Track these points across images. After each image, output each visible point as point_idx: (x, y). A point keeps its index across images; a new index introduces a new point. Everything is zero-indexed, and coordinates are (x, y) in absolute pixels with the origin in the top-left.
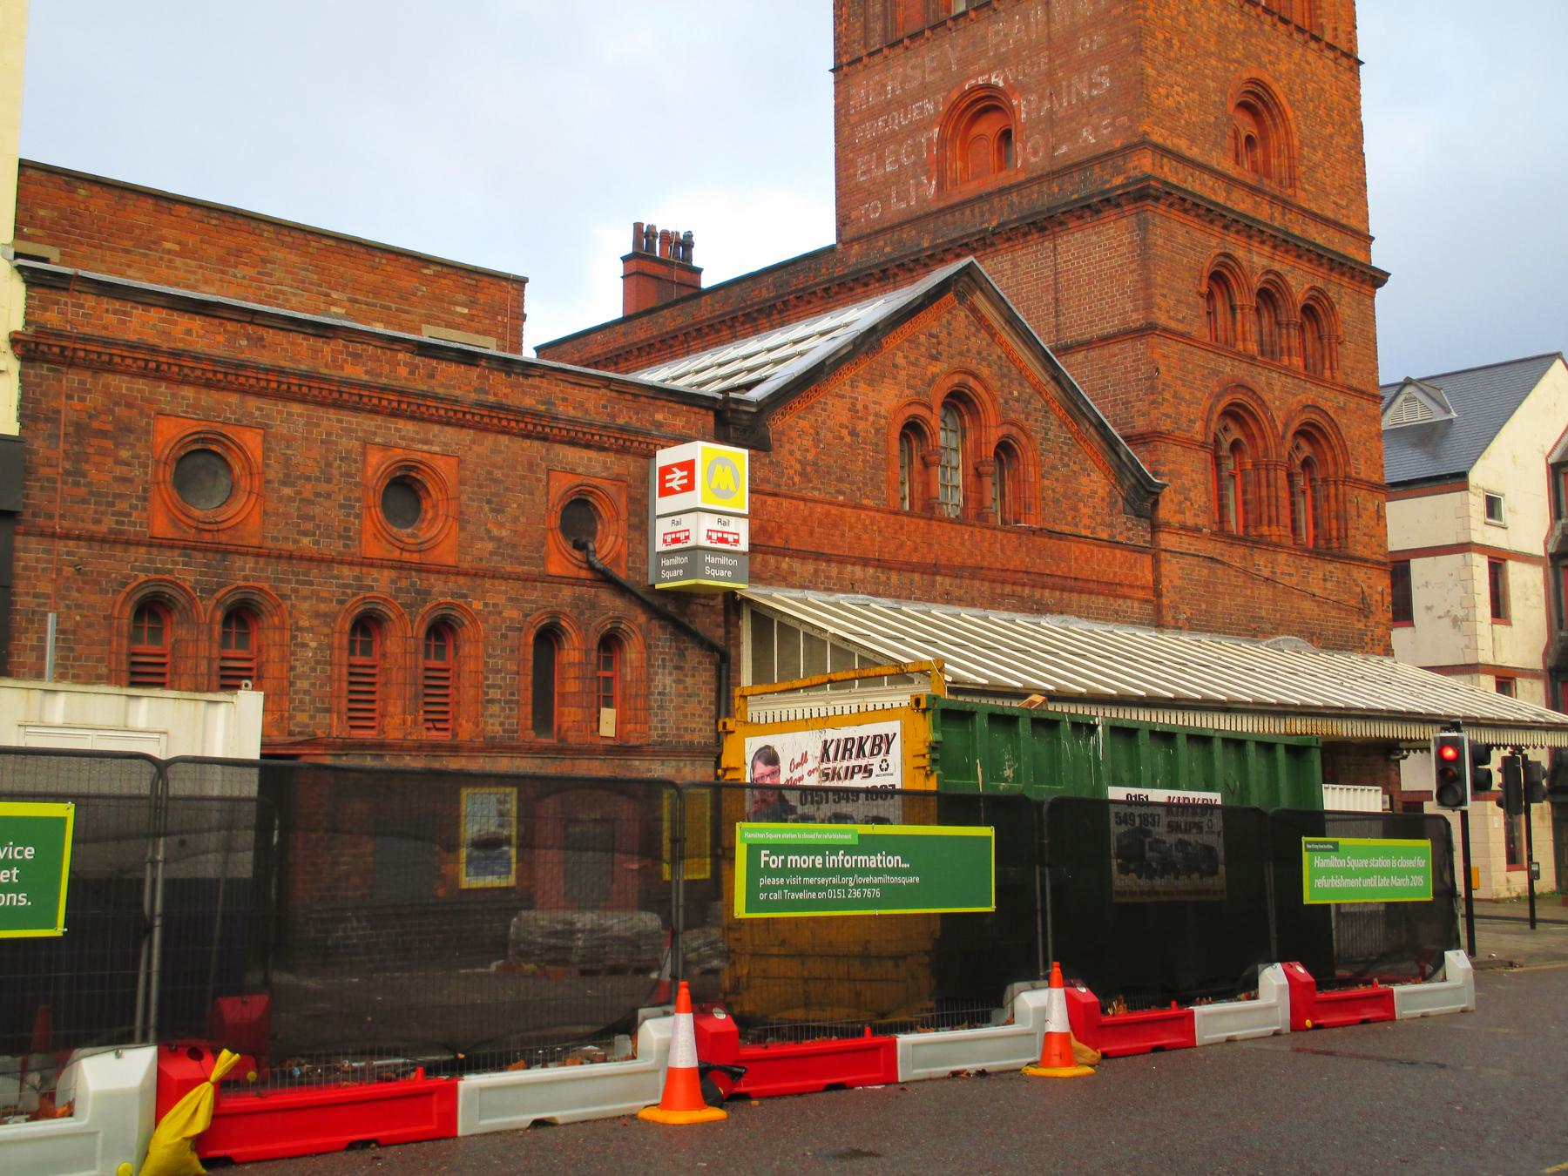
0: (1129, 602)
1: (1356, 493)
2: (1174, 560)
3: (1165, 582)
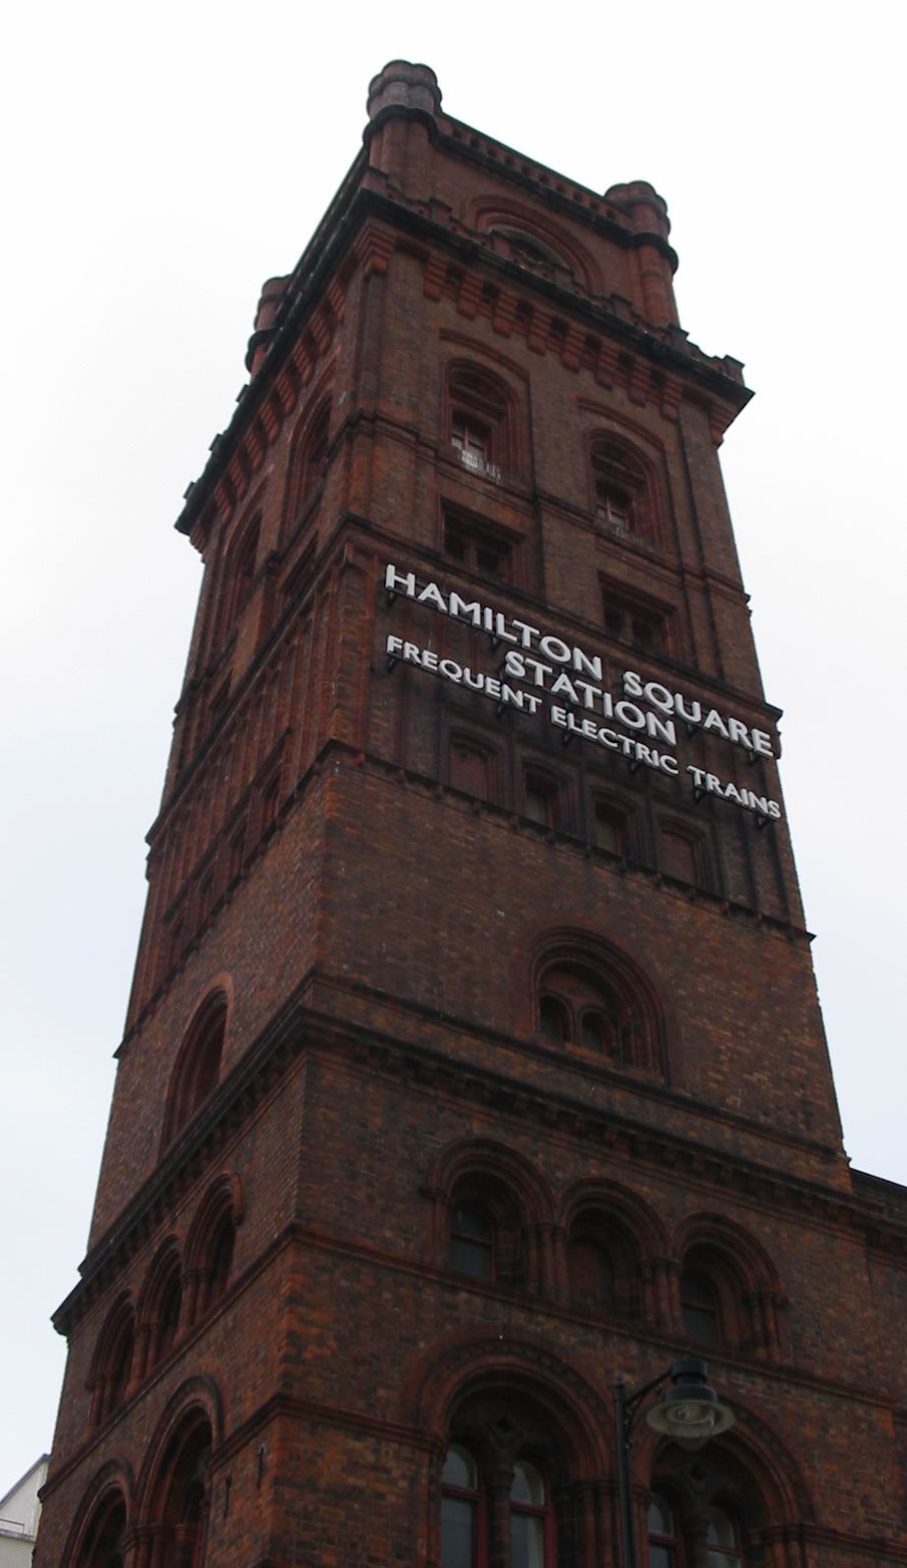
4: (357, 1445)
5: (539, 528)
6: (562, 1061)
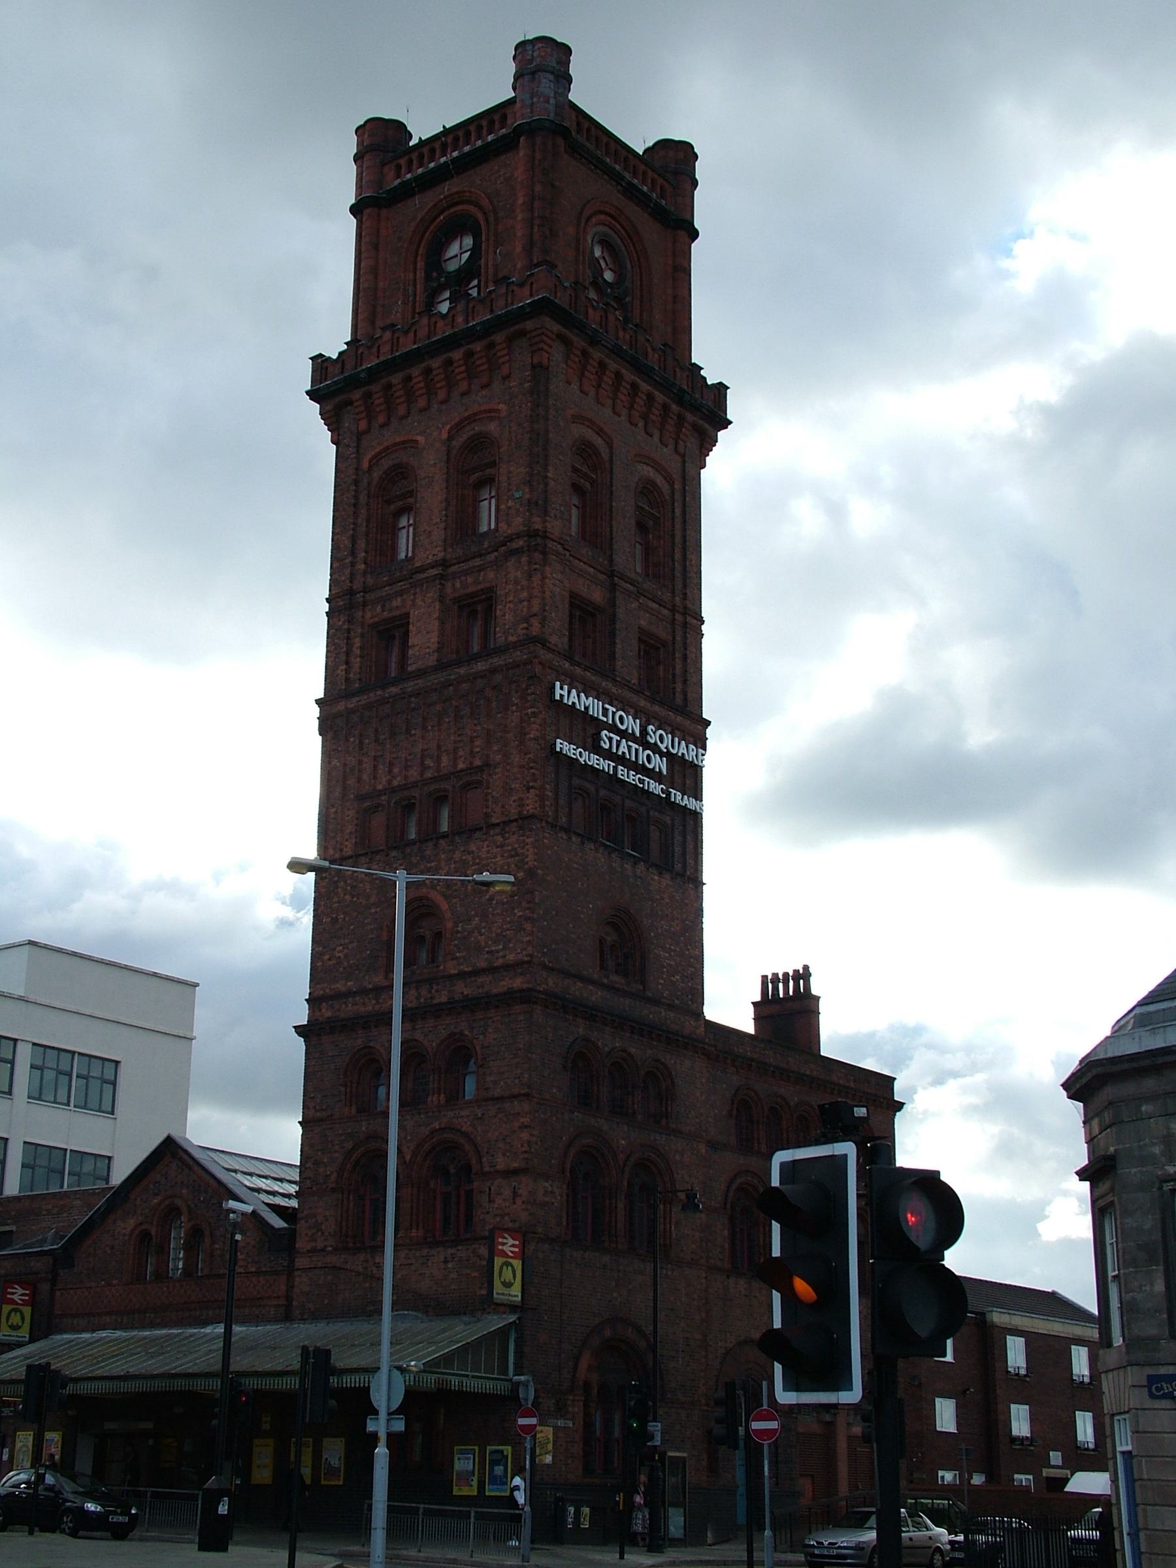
1: (489, 1184)
3: (296, 1290)
4: (546, 1184)
6: (609, 988)
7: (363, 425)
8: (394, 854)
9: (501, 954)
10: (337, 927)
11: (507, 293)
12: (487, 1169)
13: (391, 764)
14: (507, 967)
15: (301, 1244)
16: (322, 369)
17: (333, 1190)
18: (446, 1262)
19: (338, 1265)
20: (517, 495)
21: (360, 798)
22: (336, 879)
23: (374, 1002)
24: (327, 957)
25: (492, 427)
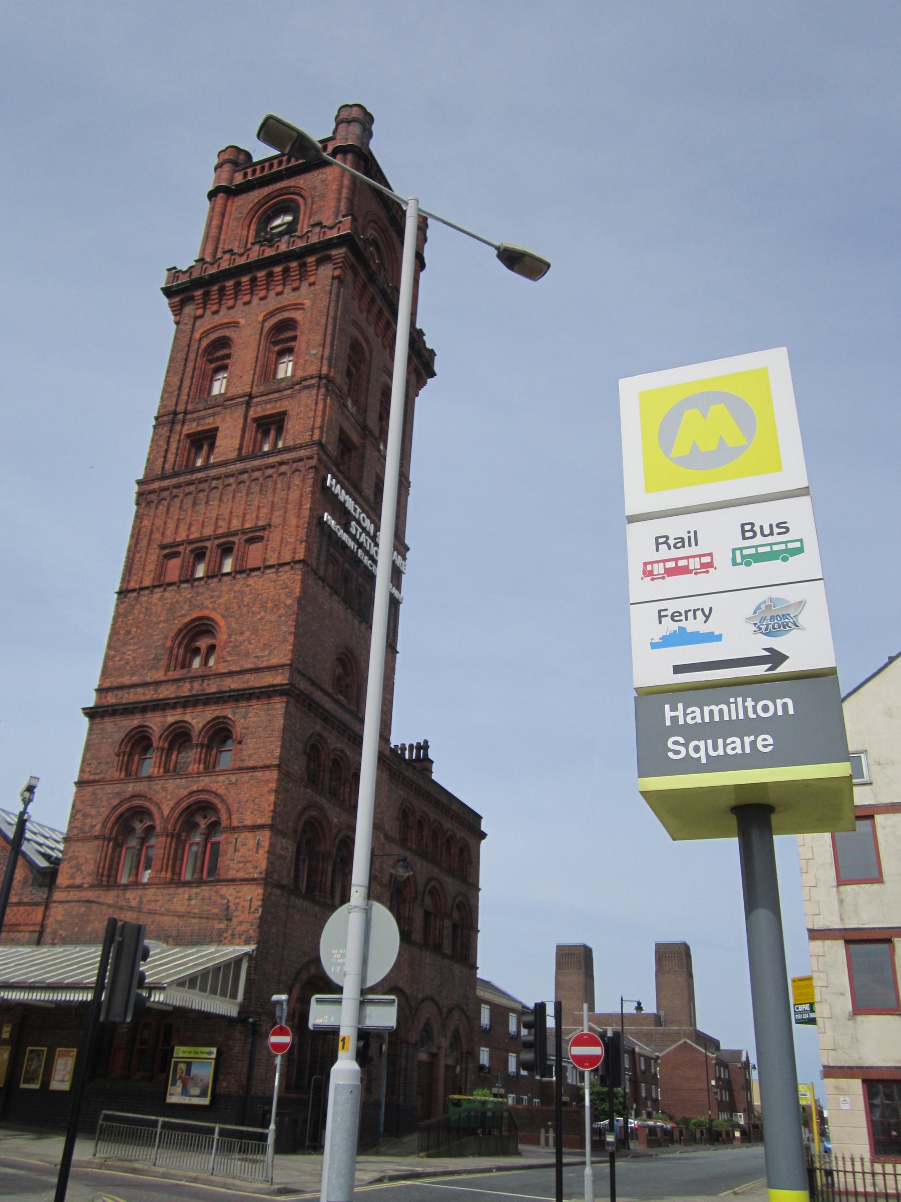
0: (22, 934)
1: (236, 836)
2: (60, 906)
5: (364, 446)
7: (200, 312)
8: (184, 586)
9: (266, 658)
10: (130, 637)
11: (320, 233)
12: (235, 823)
13: (190, 524)
14: (270, 668)
15: (62, 880)
16: (174, 276)
17: (96, 838)
18: (190, 899)
19: (92, 899)
20: (313, 352)
21: (163, 547)
22: (134, 603)
23: (153, 692)
24: (117, 659)
25: (297, 315)
